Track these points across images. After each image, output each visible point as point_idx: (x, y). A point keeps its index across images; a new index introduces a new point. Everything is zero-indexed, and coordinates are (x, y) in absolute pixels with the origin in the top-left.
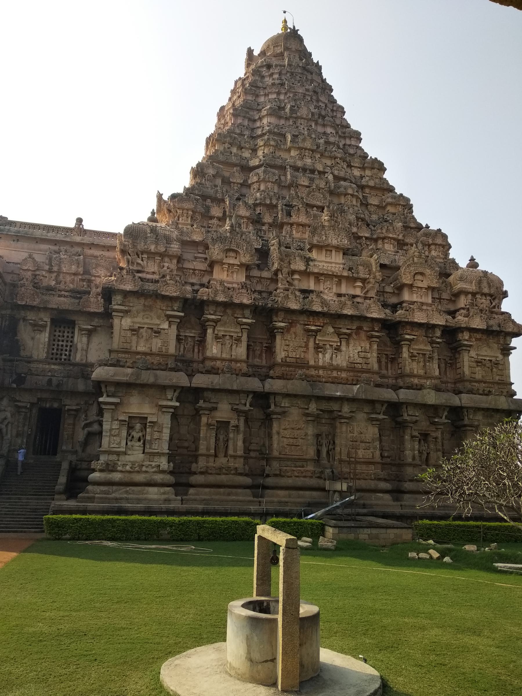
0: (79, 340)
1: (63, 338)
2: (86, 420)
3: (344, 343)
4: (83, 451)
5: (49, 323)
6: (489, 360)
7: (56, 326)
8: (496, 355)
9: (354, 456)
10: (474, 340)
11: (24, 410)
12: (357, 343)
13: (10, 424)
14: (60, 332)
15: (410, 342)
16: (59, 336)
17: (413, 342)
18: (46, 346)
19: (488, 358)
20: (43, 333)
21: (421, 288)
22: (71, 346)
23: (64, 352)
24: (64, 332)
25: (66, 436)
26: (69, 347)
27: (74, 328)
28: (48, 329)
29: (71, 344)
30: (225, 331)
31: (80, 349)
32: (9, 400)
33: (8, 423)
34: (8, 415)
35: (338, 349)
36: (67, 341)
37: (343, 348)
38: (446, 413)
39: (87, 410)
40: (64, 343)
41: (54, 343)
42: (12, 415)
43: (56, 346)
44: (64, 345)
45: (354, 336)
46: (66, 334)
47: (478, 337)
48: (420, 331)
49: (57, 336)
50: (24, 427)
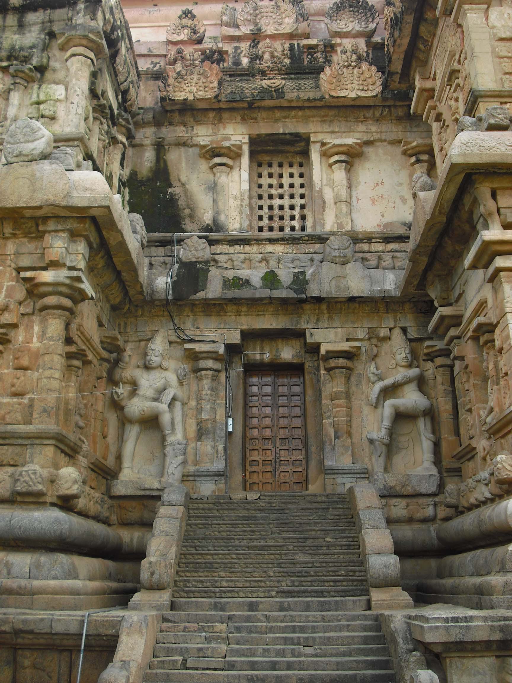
0: (325, 182)
1: (280, 191)
2: (381, 379)
4: (386, 469)
5: (246, 149)
7: (260, 165)
11: (210, 363)
13: (178, 405)
14: (271, 176)
16: (270, 186)
18: (247, 202)
20: (235, 173)
22: (303, 207)
23: (287, 222)
24: (281, 176)
25: (331, 431)
26: (298, 209)
27: (306, 153)
28: (245, 160)
29: (302, 201)
31: (332, 201)
32: (171, 343)
33: (174, 399)
34: (173, 378)
36: (292, 196)
39: (376, 356)
40: (286, 202)
41: (260, 202)
42: (181, 382)
43: (266, 209)
44: (287, 207)
46: (286, 181)
49: (265, 187)
50: (214, 409)
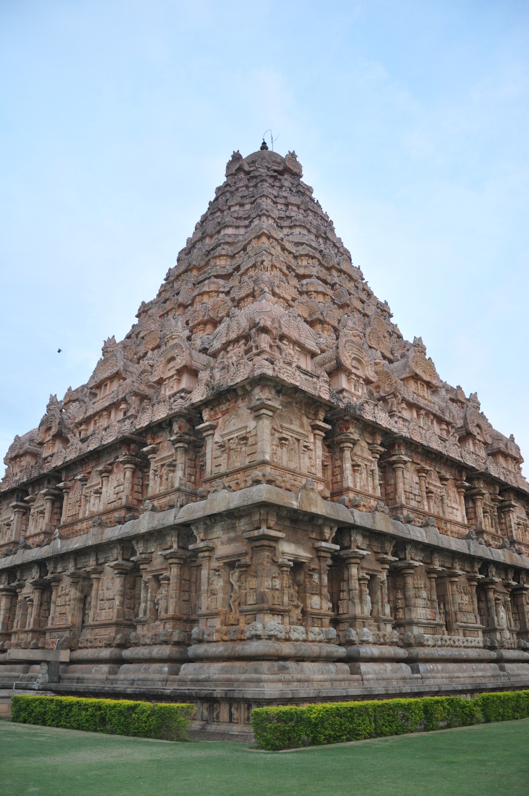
3: (104, 484)
6: (237, 437)
8: (245, 425)
9: (98, 618)
10: (220, 415)
12: (115, 477)
15: (155, 453)
17: (158, 453)
19: (236, 435)
21: (172, 376)
30: (37, 507)
35: (98, 492)
37: (104, 490)
38: (175, 539)
45: (115, 470)
47: (224, 409)
48: (164, 434)
